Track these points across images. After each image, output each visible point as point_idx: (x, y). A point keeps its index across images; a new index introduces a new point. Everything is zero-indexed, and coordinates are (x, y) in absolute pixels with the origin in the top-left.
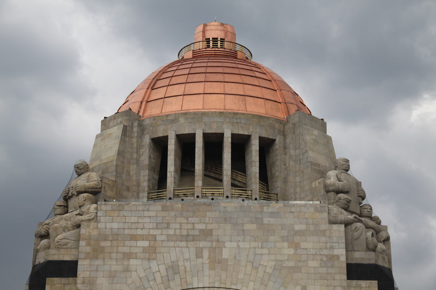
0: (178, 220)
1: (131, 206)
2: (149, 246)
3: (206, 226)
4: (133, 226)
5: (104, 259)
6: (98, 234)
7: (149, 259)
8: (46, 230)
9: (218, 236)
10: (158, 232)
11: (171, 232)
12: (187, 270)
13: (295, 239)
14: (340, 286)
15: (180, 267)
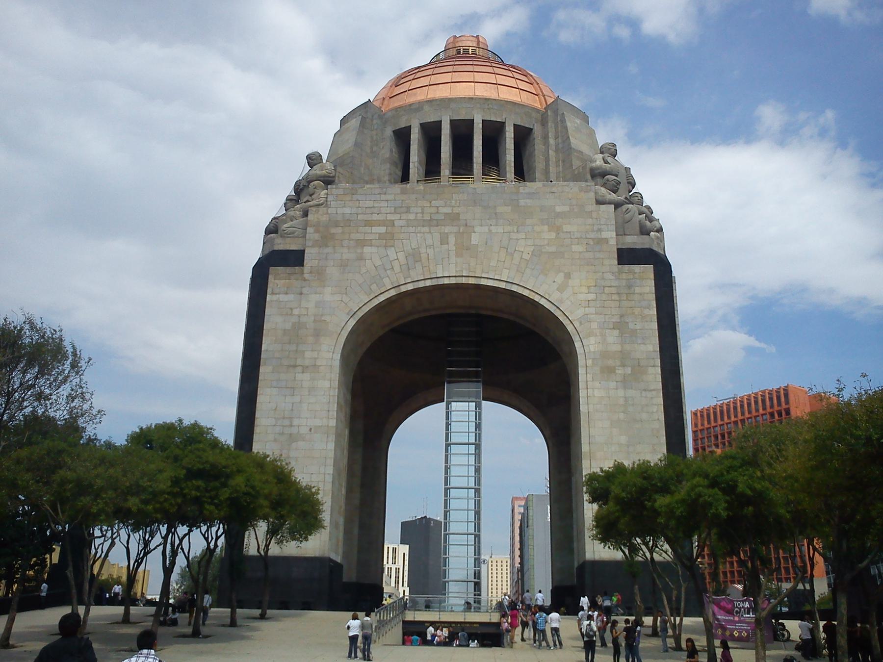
0: (420, 203)
1: (365, 190)
2: (386, 233)
3: (452, 210)
4: (368, 211)
5: (334, 247)
6: (328, 219)
7: (386, 247)
8: (275, 225)
9: (466, 220)
10: (398, 216)
11: (412, 217)
12: (430, 258)
13: (556, 222)
14: (610, 272)
15: (422, 255)
